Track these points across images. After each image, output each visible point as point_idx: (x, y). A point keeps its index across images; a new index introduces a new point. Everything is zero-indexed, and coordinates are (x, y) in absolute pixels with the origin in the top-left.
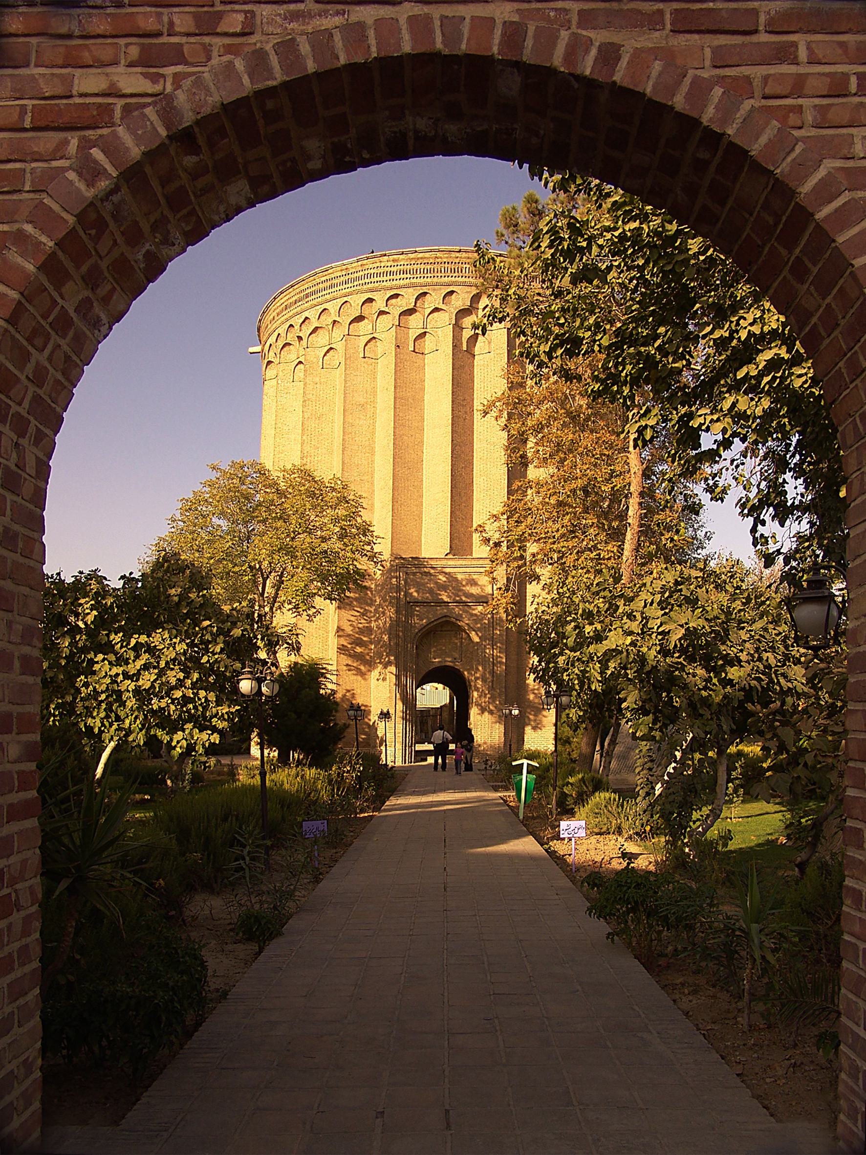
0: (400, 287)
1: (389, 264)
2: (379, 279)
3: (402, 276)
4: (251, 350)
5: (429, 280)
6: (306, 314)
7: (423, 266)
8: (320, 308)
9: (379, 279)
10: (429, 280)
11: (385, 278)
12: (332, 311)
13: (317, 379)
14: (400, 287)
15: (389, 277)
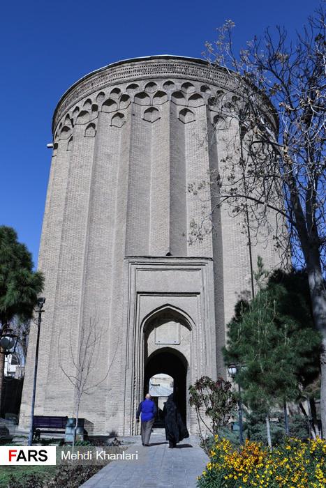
0: (135, 80)
1: (129, 67)
2: (122, 76)
3: (138, 73)
4: (49, 145)
5: (154, 75)
6: (77, 105)
7: (150, 68)
8: (85, 100)
9: (122, 76)
10: (154, 75)
11: (126, 75)
12: (92, 100)
13: (81, 144)
14: (135, 80)
15: (128, 75)
